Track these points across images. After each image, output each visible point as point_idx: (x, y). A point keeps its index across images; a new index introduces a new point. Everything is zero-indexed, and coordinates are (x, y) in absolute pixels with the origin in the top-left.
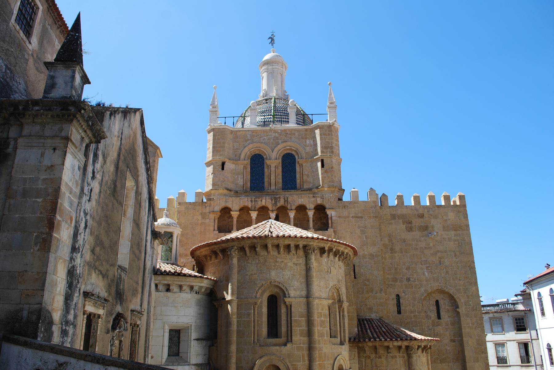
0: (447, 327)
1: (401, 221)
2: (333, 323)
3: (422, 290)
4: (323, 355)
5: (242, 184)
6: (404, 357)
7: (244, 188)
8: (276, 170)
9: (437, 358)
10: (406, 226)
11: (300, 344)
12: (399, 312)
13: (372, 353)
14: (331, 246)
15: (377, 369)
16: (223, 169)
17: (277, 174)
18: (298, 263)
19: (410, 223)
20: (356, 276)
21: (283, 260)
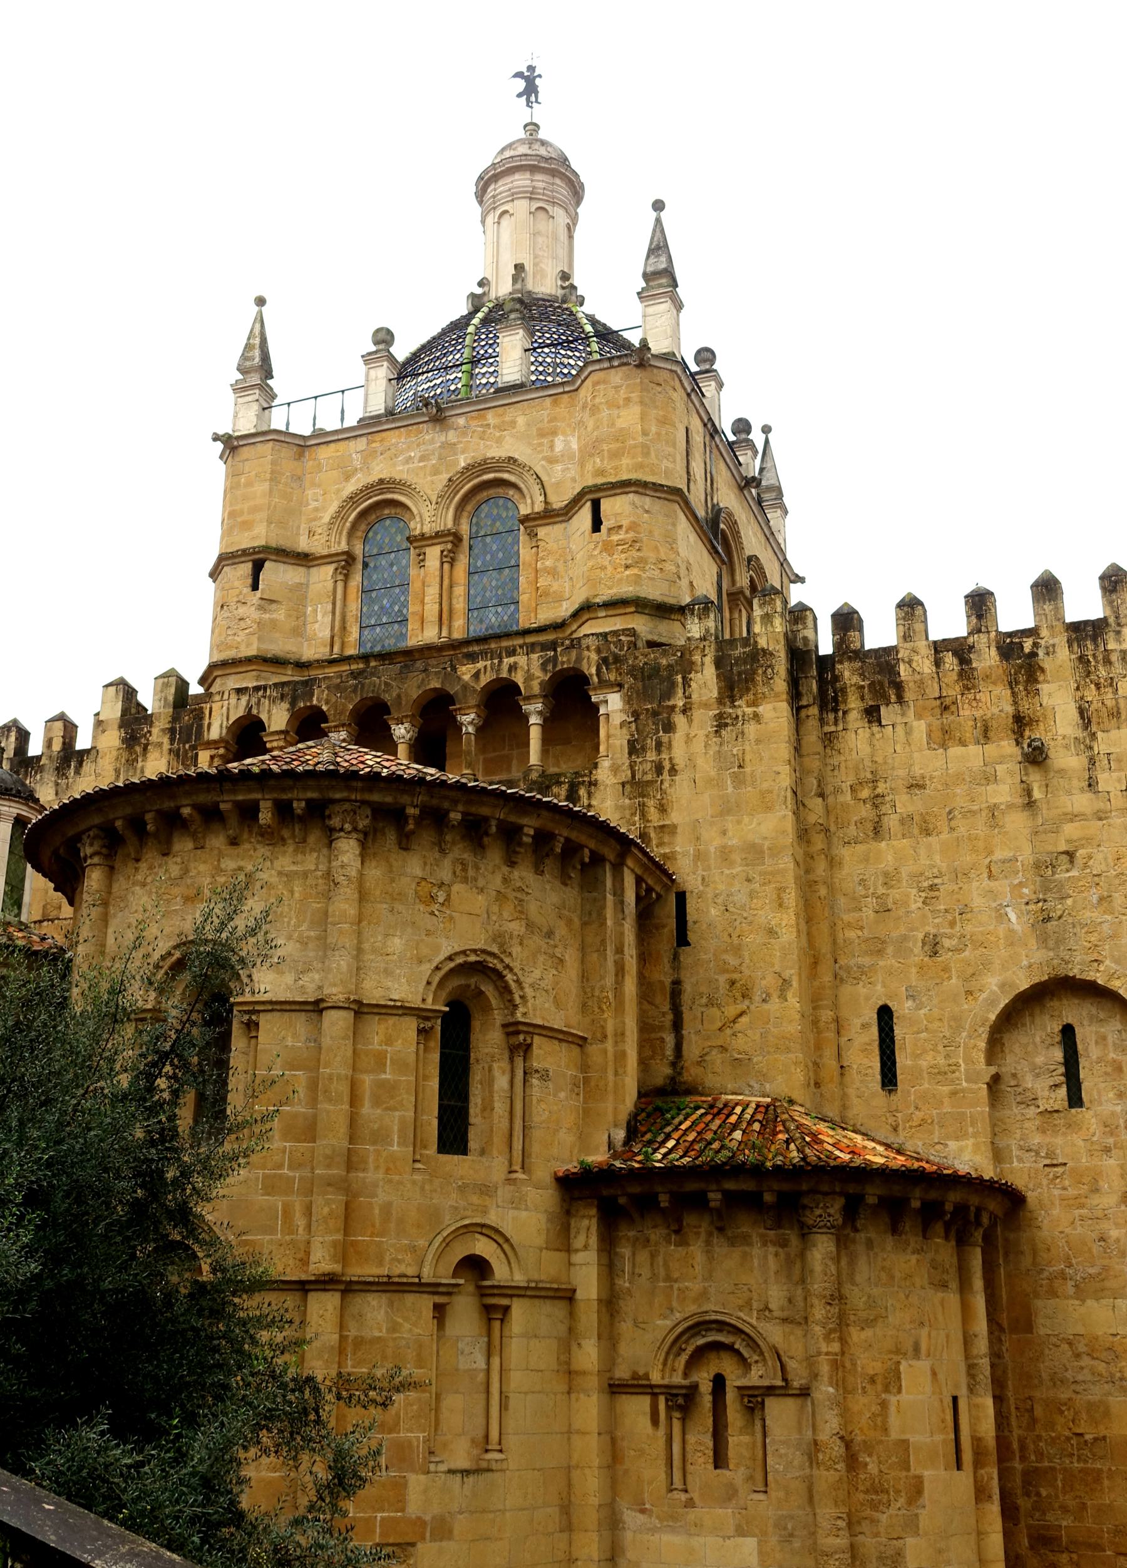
0: (1111, 1140)
2: (479, 1101)
3: (992, 982)
4: (377, 1211)
5: (327, 633)
6: (783, 1243)
7: (336, 649)
9: (1062, 1272)
10: (929, 725)
11: (280, 1166)
12: (889, 1077)
13: (655, 1227)
14: (435, 802)
15: (672, 1287)
16: (255, 587)
18: (296, 873)
20: (691, 937)
21: (242, 863)
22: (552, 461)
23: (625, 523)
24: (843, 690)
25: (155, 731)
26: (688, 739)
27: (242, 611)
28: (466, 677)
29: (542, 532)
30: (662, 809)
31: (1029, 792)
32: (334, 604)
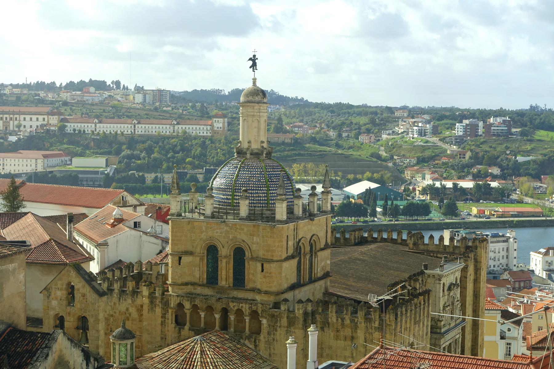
8: (227, 265)
10: (334, 334)
16: (180, 264)
17: (227, 269)
22: (253, 243)
23: (269, 271)
24: (317, 321)
25: (157, 301)
26: (280, 334)
28: (232, 306)
30: (274, 349)
31: (352, 354)
32: (200, 268)
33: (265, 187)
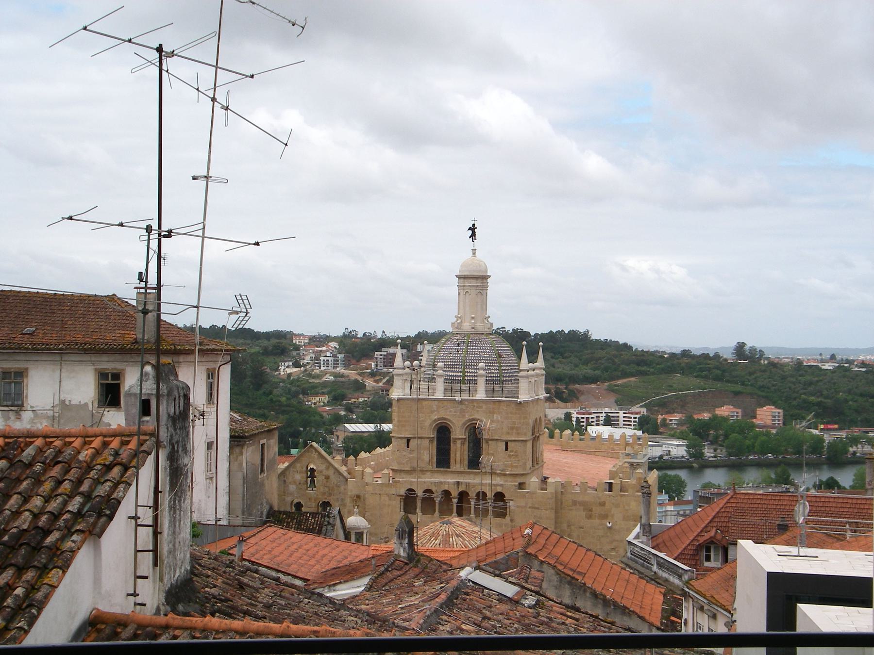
1: (582, 508)
5: (428, 460)
16: (408, 447)
19: (591, 510)
27: (404, 453)
29: (490, 442)
33: (497, 363)
